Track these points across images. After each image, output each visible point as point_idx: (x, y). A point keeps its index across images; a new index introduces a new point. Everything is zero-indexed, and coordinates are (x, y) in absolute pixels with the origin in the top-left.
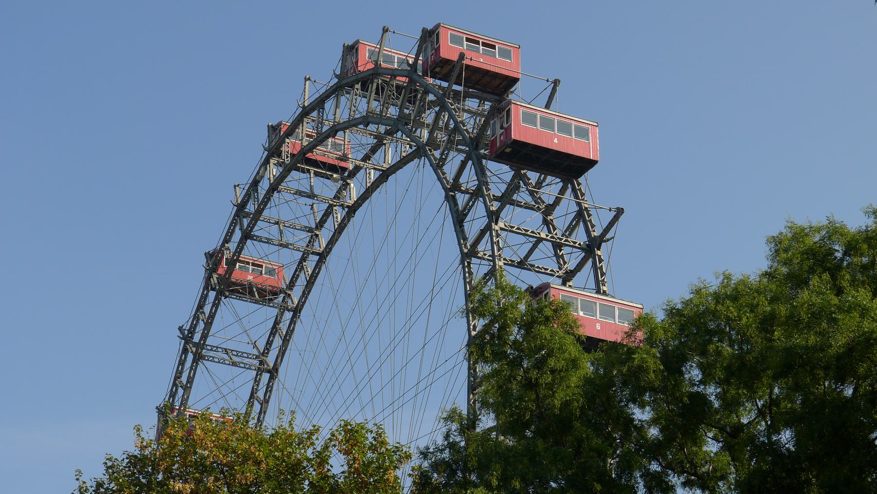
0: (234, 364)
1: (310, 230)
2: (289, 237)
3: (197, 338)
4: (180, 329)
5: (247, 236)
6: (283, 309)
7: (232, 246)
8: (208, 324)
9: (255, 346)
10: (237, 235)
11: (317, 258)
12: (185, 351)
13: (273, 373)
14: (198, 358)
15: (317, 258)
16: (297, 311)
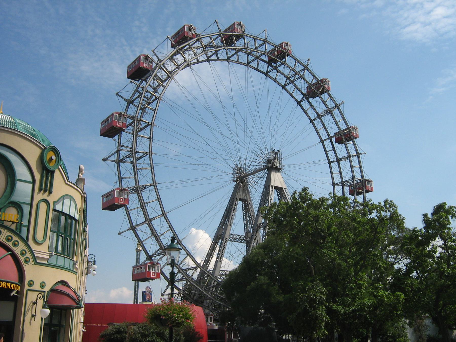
8: (352, 167)
13: (330, 163)
16: (334, 185)
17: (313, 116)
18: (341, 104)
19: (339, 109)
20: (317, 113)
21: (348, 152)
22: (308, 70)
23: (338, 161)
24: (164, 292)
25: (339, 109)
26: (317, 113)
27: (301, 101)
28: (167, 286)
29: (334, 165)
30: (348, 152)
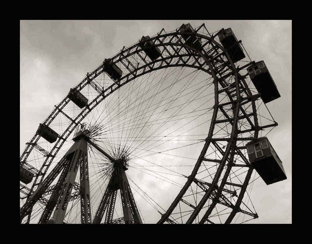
0: (96, 89)
1: (135, 69)
2: (130, 67)
3: (90, 78)
4: (88, 73)
5: (120, 60)
6: (116, 83)
7: (114, 61)
9: (103, 88)
10: (118, 58)
11: (133, 76)
12: (86, 79)
13: (104, 97)
14: (89, 83)
15: (133, 76)
16: (120, 86)
17: (74, 125)
18: (56, 107)
19: (59, 106)
20: (72, 124)
21: (86, 84)
22: (32, 141)
23: (103, 92)
24: (250, 214)
25: (59, 106)
26: (72, 124)
27: (63, 139)
28: (242, 212)
29: (105, 94)
30: (86, 84)
